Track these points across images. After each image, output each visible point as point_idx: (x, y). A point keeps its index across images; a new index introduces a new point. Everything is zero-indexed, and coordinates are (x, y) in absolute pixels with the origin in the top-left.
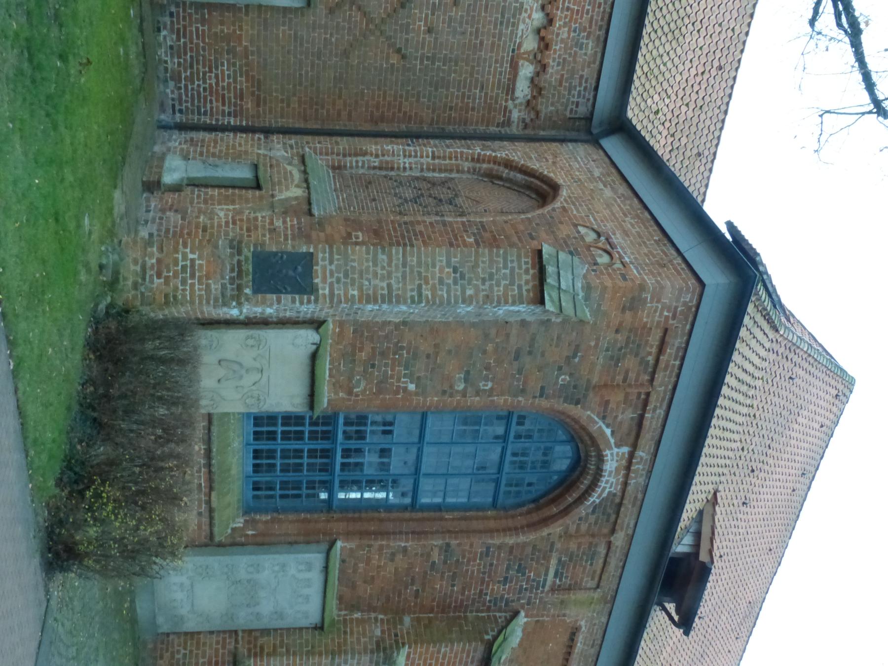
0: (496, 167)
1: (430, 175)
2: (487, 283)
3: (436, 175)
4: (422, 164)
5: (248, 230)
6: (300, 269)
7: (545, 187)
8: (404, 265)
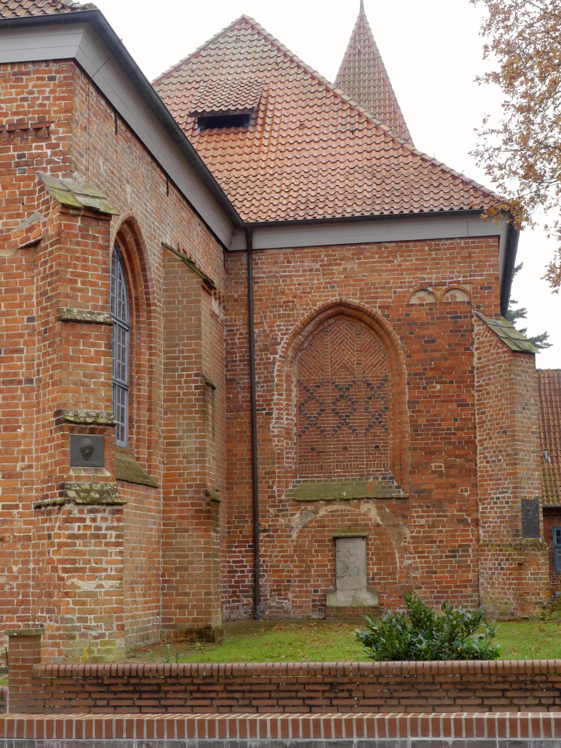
0: (293, 344)
1: (294, 401)
2: (529, 389)
3: (294, 394)
4: (287, 405)
5: (434, 542)
6: (528, 508)
7: (329, 312)
8: (523, 441)
